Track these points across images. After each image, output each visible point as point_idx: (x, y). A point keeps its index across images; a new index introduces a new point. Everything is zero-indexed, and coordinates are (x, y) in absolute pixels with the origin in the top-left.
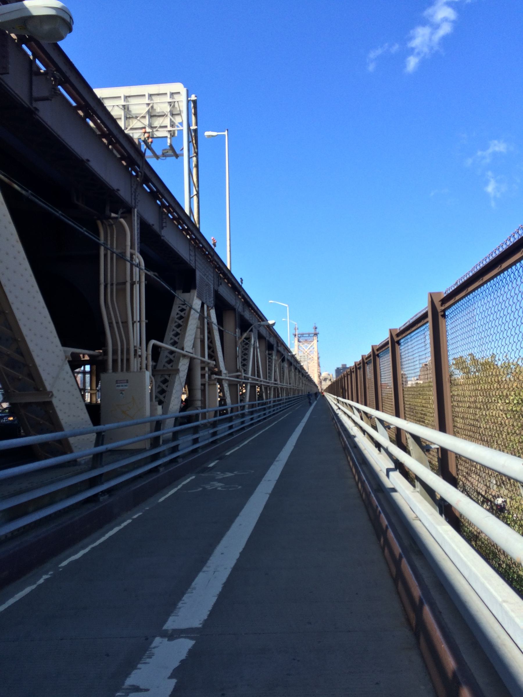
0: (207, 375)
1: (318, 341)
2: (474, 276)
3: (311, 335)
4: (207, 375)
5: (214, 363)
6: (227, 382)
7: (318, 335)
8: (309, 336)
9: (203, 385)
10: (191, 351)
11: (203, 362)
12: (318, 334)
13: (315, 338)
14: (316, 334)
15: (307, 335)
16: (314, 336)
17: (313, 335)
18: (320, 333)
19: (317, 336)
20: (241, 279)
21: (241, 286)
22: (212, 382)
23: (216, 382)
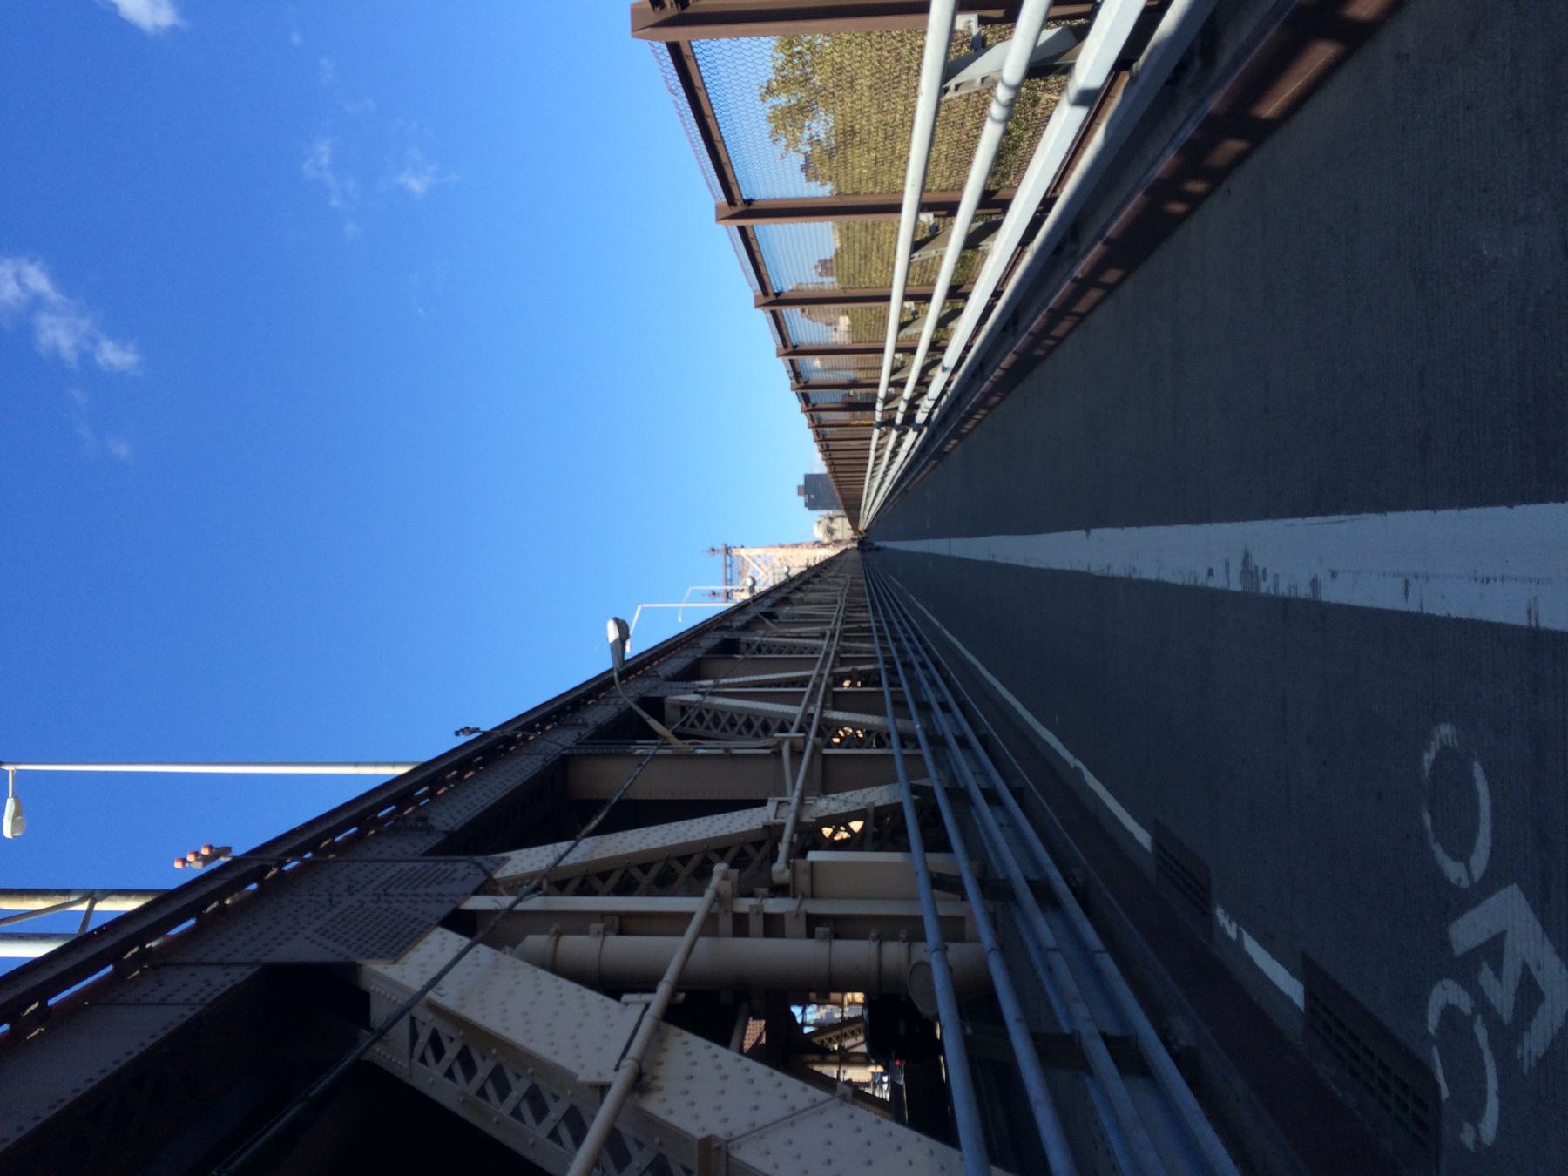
0: (773, 905)
4: (773, 905)
5: (720, 868)
6: (809, 800)
9: (813, 924)
10: (634, 1012)
11: (710, 926)
20: (457, 733)
21: (486, 734)
22: (803, 881)
23: (799, 861)
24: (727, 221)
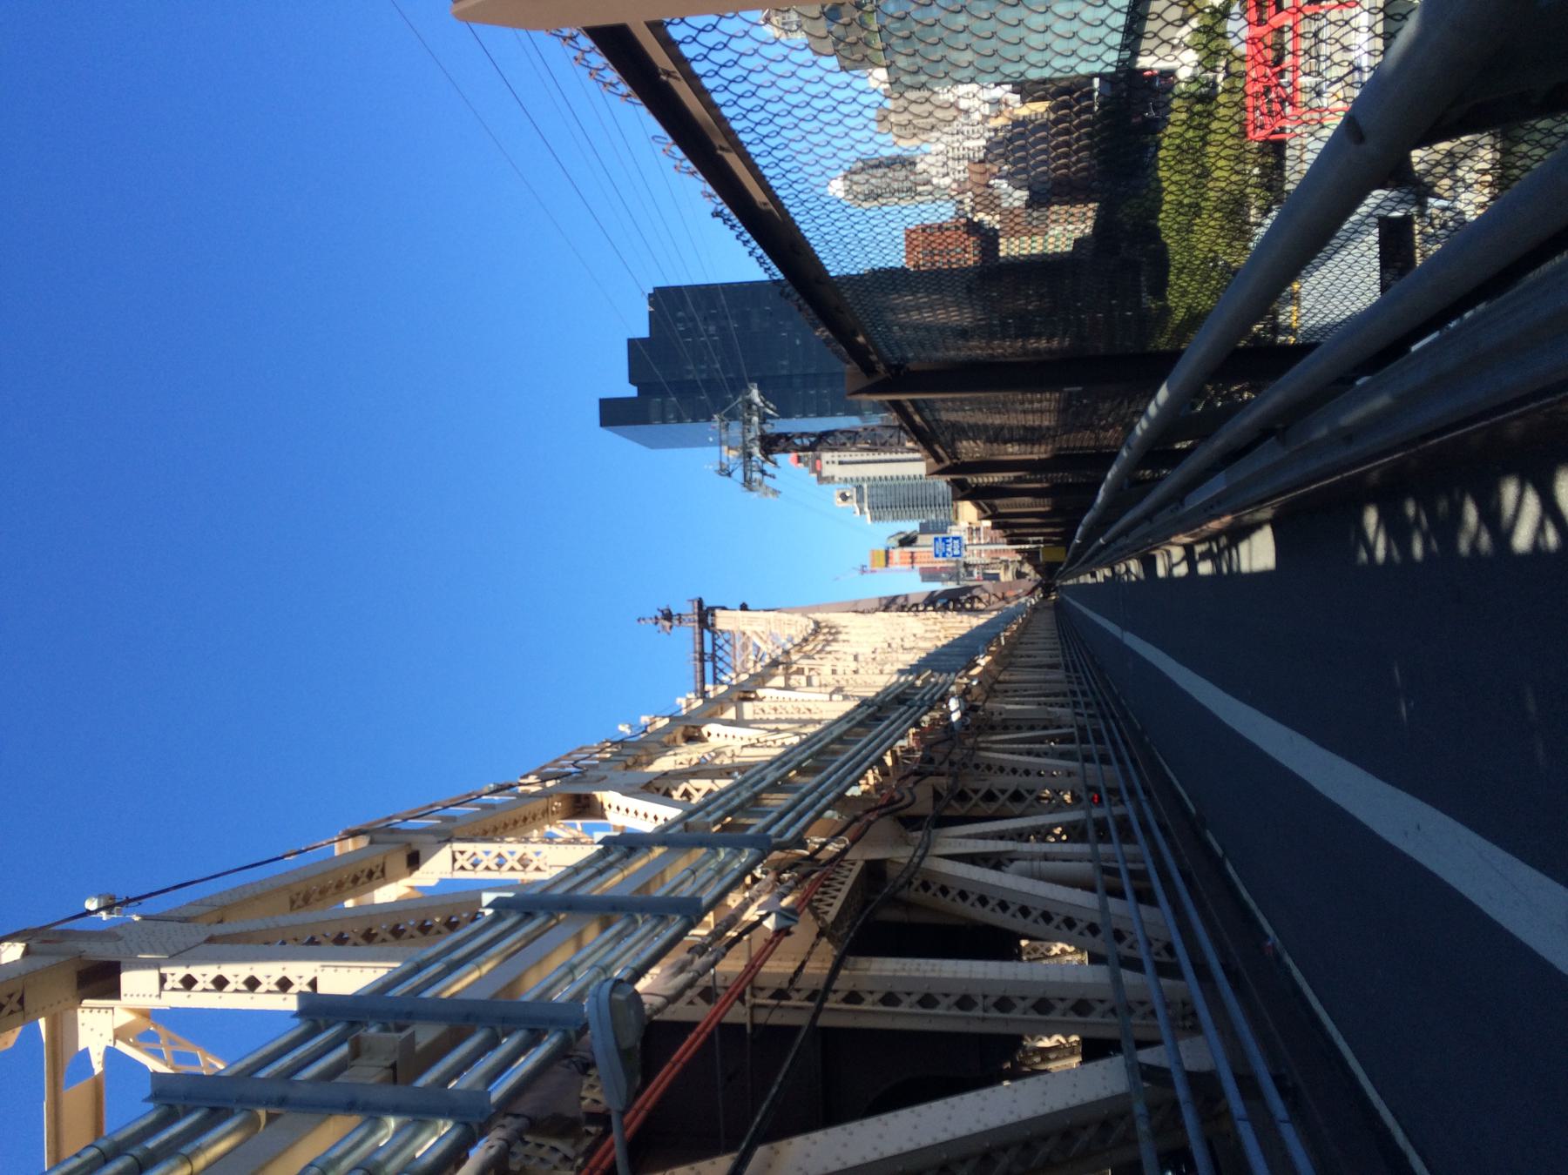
1: (744, 608)
2: (710, 178)
3: (708, 649)
7: (707, 603)
8: (714, 656)
12: (700, 602)
13: (723, 621)
14: (705, 616)
15: (709, 666)
16: (714, 633)
17: (707, 635)
18: (696, 596)
19: (712, 609)
24: (936, 476)
